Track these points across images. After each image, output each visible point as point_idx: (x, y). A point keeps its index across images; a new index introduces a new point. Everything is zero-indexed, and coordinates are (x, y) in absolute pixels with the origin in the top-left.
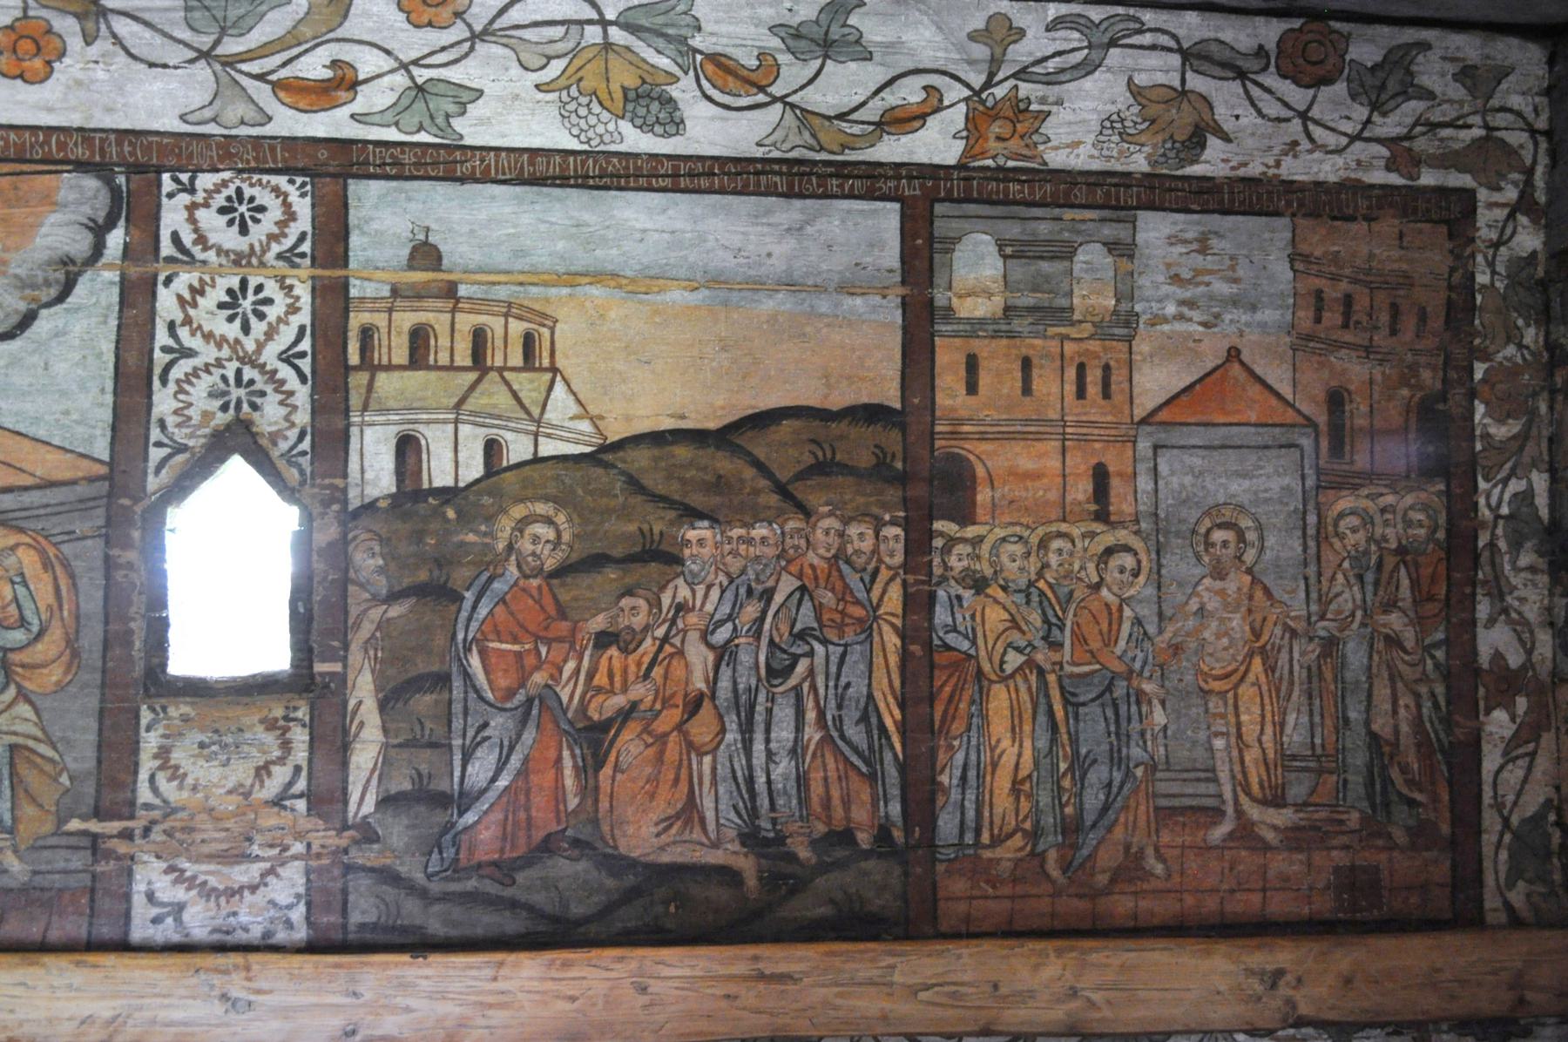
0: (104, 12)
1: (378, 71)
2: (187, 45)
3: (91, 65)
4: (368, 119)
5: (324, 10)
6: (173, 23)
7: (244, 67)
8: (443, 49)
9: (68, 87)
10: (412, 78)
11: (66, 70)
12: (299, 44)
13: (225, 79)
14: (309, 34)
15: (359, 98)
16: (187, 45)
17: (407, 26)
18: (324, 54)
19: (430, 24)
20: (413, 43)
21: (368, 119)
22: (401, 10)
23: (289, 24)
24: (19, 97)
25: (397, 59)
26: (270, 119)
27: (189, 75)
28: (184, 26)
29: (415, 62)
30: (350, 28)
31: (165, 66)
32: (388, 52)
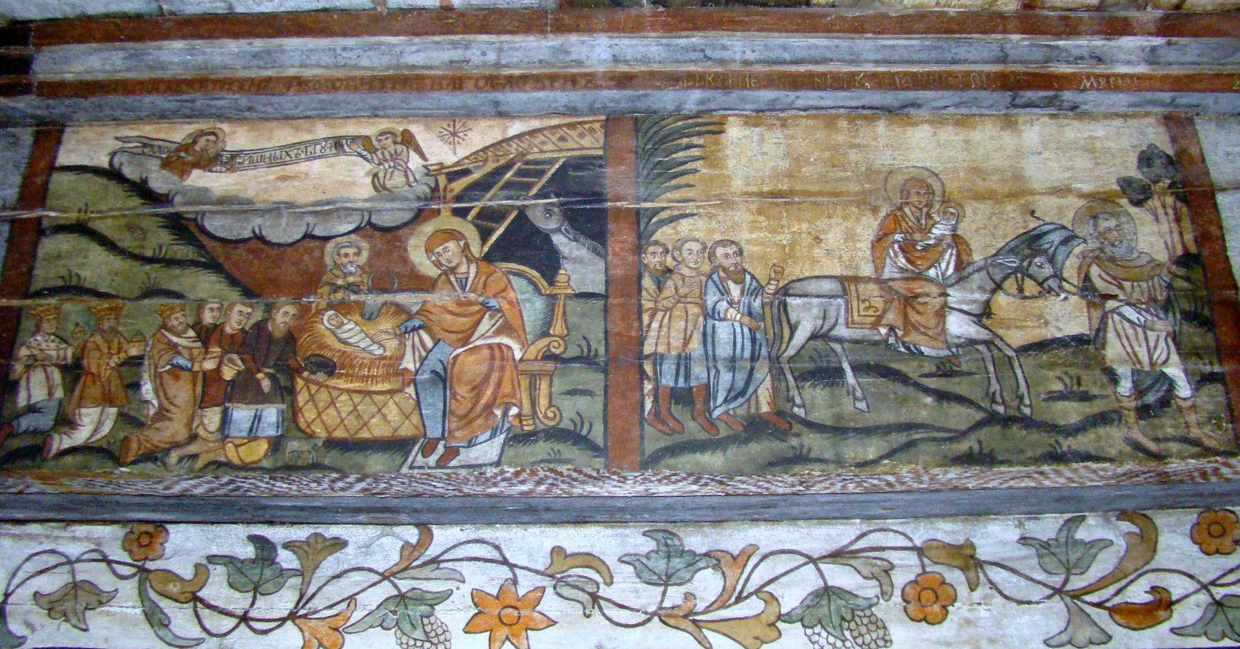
0: (980, 564)
1: (1186, 592)
2: (1045, 585)
3: (975, 606)
4: (1183, 631)
5: (1140, 548)
6: (1032, 569)
7: (1088, 598)
8: (1231, 571)
9: (960, 625)
10: (1212, 595)
11: (958, 612)
12: (1126, 576)
13: (1073, 608)
14: (1132, 568)
15: (1175, 615)
16: (1045, 585)
17: (1201, 555)
18: (1144, 583)
19: (1217, 552)
20: (1210, 567)
21: (1183, 631)
22: (1195, 543)
23: (1115, 561)
24: (925, 636)
25: (1198, 581)
26: (1110, 637)
27: (1050, 608)
28: (1040, 570)
29: (1213, 583)
30: (1161, 560)
31: (1029, 603)
32: (1191, 577)
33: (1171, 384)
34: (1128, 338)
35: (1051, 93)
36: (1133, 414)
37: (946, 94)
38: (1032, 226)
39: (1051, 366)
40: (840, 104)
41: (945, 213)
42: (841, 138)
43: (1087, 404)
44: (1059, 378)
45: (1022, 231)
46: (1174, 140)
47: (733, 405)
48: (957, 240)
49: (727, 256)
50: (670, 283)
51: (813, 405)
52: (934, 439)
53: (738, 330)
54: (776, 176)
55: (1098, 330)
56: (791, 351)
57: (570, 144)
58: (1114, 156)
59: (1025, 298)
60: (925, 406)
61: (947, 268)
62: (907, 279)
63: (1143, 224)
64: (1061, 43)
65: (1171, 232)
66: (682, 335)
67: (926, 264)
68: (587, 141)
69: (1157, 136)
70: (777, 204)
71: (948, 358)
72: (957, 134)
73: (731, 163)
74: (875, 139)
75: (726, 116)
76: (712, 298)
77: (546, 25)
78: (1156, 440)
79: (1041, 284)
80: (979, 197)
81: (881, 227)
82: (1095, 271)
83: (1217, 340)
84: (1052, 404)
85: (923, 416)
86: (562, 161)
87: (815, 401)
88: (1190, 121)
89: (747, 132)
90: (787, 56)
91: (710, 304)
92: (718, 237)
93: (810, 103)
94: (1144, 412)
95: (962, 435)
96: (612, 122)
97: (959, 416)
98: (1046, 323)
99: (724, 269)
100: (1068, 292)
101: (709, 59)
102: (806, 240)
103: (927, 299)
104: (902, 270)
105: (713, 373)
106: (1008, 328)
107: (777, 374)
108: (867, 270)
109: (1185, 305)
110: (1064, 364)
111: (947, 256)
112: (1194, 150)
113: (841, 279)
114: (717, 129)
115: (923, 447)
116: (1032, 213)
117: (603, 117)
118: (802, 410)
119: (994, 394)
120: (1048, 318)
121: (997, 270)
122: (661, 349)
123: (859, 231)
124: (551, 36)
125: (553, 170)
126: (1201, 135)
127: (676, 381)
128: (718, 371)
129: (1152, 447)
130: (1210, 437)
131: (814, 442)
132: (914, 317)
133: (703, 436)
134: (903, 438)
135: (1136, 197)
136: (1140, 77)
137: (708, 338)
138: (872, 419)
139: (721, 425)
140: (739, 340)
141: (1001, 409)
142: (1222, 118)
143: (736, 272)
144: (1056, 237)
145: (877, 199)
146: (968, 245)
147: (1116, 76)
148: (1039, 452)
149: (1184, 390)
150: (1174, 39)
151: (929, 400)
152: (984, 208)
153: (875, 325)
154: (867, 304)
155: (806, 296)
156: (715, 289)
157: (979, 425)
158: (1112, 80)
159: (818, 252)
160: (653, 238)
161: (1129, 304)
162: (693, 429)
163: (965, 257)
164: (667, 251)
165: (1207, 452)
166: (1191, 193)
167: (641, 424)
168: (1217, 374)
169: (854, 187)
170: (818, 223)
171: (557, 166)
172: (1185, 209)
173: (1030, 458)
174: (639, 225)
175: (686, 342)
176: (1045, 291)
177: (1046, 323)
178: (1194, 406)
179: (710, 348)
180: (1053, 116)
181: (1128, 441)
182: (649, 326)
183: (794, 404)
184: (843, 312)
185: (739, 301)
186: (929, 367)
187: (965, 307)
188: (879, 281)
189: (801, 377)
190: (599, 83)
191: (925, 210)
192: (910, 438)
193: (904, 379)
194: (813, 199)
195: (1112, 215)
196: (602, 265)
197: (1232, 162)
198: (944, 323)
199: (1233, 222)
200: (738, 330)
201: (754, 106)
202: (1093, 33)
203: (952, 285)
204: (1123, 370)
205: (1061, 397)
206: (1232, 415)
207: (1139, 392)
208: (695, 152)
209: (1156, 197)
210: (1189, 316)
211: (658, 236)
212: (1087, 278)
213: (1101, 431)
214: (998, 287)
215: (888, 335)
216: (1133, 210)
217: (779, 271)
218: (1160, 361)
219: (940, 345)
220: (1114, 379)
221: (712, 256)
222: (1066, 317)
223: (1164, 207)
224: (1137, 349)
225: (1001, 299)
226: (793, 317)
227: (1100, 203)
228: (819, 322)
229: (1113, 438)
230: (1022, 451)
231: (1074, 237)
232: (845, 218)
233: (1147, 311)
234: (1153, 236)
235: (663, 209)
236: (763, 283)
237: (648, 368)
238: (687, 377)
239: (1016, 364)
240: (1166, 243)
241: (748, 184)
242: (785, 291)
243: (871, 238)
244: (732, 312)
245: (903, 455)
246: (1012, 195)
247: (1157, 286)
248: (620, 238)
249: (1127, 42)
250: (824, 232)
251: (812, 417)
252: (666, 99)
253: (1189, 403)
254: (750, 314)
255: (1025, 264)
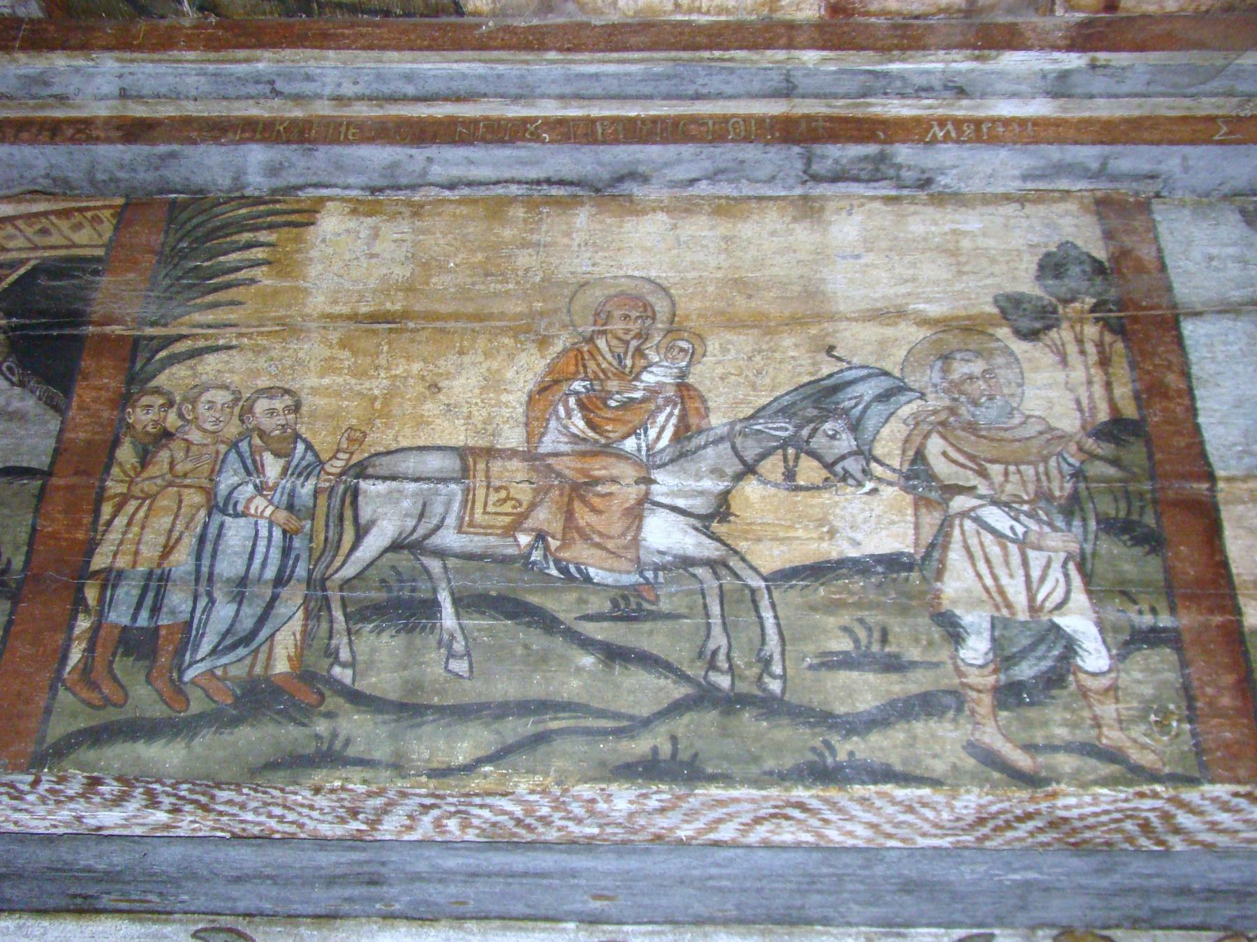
33: (1070, 647)
34: (988, 561)
35: (872, 149)
36: (987, 699)
37: (687, 150)
38: (825, 371)
39: (833, 607)
40: (507, 175)
41: (669, 349)
42: (507, 233)
43: (894, 677)
44: (846, 629)
45: (806, 379)
46: (1108, 235)
47: (224, 660)
48: (684, 390)
49: (272, 412)
50: (164, 455)
51: (370, 664)
52: (588, 732)
53: (264, 532)
54: (386, 290)
55: (932, 546)
56: (349, 571)
57: (55, 239)
58: (993, 261)
59: (798, 488)
60: (579, 670)
61: (658, 438)
62: (584, 454)
63: (1037, 369)
64: (895, 67)
65: (1090, 383)
66: (162, 540)
67: (623, 429)
68: (82, 237)
69: (1081, 231)
70: (374, 332)
71: (634, 588)
72: (712, 228)
73: (313, 271)
74: (568, 234)
75: (322, 200)
76: (227, 481)
77: (15, 39)
78: (1030, 748)
79: (829, 466)
80: (733, 323)
81: (551, 369)
82: (935, 445)
83: (1168, 570)
84: (823, 673)
85: (572, 687)
86: (33, 263)
87: (379, 658)
88: (1144, 207)
89: (352, 224)
90: (410, 90)
91: (223, 489)
92: (263, 382)
93: (456, 172)
94: (1010, 695)
95: (637, 726)
96: (134, 207)
97: (641, 691)
98: (832, 533)
99: (262, 434)
100: (880, 480)
101: (278, 94)
102: (415, 389)
103: (614, 488)
104: (576, 439)
105: (202, 602)
106: (759, 540)
107: (317, 608)
108: (513, 438)
109: (1107, 506)
110: (859, 605)
111: (661, 418)
112: (1146, 253)
113: (462, 453)
114: (306, 217)
115: (559, 744)
116: (830, 350)
117: (120, 201)
118: (349, 672)
119: (715, 653)
120: (838, 524)
121: (750, 442)
122: (121, 563)
123: (510, 374)
124: (22, 57)
125: (14, 277)
126: (1162, 229)
127: (135, 617)
128: (212, 601)
129: (1022, 760)
130: (1144, 747)
131: (358, 729)
132: (584, 517)
133: (159, 711)
134: (528, 726)
135: (1025, 324)
136: (1036, 122)
137: (207, 544)
138: (473, 691)
139: (195, 694)
140: (261, 549)
141: (724, 681)
142: (1207, 201)
143: (280, 439)
144: (868, 390)
145: (551, 324)
146: (704, 400)
147: (994, 121)
148: (789, 762)
149: (1094, 657)
150: (1102, 56)
151: (588, 661)
152: (743, 342)
153: (511, 530)
154: (503, 494)
155: (394, 478)
156: (238, 465)
157: (676, 708)
158: (984, 128)
159: (430, 408)
160: (153, 383)
161: (995, 503)
162: (144, 698)
163: (693, 420)
164: (171, 404)
165: (1139, 774)
166: (1135, 320)
167: (53, 689)
168: (1164, 630)
169: (515, 307)
170: (441, 362)
171: (22, 271)
172: (1120, 346)
173: (771, 773)
174: (133, 362)
175: (167, 550)
176: (835, 473)
177: (832, 533)
178: (1113, 689)
179: (206, 562)
180: (888, 200)
181: (973, 748)
182: (109, 523)
183: (337, 661)
184: (456, 506)
185: (274, 489)
186: (600, 604)
187: (681, 503)
188: (530, 457)
189: (361, 614)
190: (95, 133)
191: (634, 343)
192: (540, 728)
193: (547, 623)
194: (439, 324)
195: (979, 354)
196: (54, 424)
197: (1217, 269)
198: (639, 528)
199: (1212, 368)
200: (264, 532)
201: (363, 180)
202: (948, 48)
203: (663, 465)
204: (975, 620)
205: (846, 662)
206: (1191, 707)
207: (1003, 657)
208: (259, 254)
209: (1065, 325)
210: (1109, 526)
211: (162, 380)
212: (920, 457)
213: (919, 727)
214: (749, 469)
215: (532, 547)
216: (1020, 347)
217: (356, 437)
218: (1049, 605)
219: (625, 565)
220: (954, 633)
221: (248, 410)
222: (875, 523)
223: (1080, 341)
224: (1004, 580)
225: (751, 489)
226: (366, 513)
227: (959, 334)
228: (410, 523)
229: (943, 741)
230: (756, 760)
231: (902, 389)
232: (487, 355)
233: (1032, 515)
234: (1055, 390)
235: (181, 337)
236: (324, 456)
237: (91, 594)
238: (155, 610)
239: (764, 603)
240: (1078, 402)
241: (335, 302)
242: (361, 470)
243: (530, 386)
244: (260, 502)
245: (522, 759)
246: (796, 322)
247: (1054, 472)
248: (97, 383)
249: (1012, 61)
250: (448, 375)
251: (361, 685)
252: (210, 165)
253: (1105, 682)
254: (290, 507)
255: (805, 432)
